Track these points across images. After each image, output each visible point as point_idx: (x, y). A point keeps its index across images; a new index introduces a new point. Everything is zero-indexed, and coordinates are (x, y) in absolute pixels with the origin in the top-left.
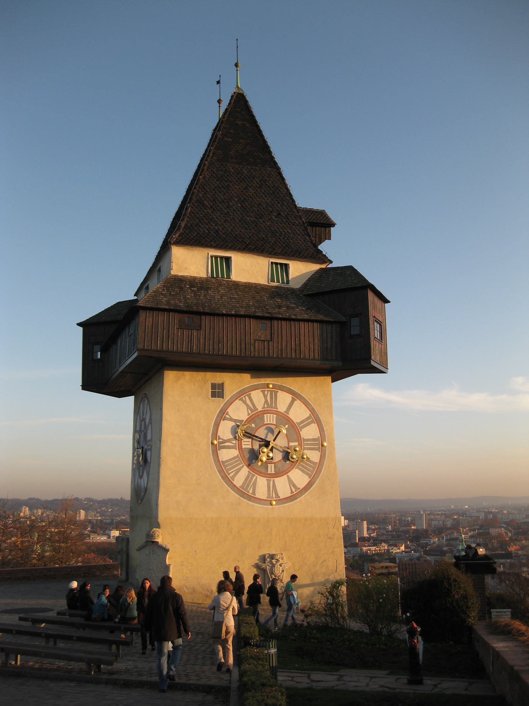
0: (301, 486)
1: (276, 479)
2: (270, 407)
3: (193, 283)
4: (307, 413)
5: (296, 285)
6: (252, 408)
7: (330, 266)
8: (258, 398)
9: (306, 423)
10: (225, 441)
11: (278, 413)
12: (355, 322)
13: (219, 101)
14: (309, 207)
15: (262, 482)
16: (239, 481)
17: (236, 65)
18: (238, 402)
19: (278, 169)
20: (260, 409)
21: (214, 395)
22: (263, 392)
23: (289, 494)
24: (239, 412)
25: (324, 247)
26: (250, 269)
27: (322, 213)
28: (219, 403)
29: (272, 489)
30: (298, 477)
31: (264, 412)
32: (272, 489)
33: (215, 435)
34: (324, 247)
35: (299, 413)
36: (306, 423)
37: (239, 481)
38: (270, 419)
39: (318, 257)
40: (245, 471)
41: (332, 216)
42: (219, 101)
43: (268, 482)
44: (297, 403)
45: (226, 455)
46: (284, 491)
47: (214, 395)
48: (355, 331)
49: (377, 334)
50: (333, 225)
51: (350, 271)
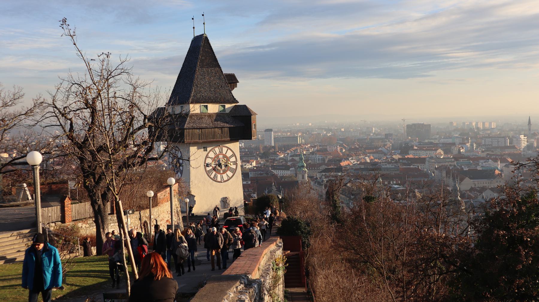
0: (230, 176)
2: (221, 152)
3: (196, 115)
4: (232, 153)
5: (227, 111)
6: (215, 154)
7: (238, 104)
8: (217, 150)
9: (231, 156)
11: (223, 154)
13: (194, 28)
14: (228, 73)
15: (219, 176)
17: (204, 24)
18: (211, 152)
19: (220, 68)
21: (204, 150)
23: (227, 179)
24: (212, 155)
25: (235, 92)
26: (214, 108)
28: (206, 153)
30: (230, 174)
34: (235, 92)
35: (229, 154)
36: (231, 156)
37: (212, 176)
38: (221, 156)
39: (234, 101)
40: (214, 173)
44: (229, 150)
46: (225, 178)
47: (204, 150)
51: (245, 107)
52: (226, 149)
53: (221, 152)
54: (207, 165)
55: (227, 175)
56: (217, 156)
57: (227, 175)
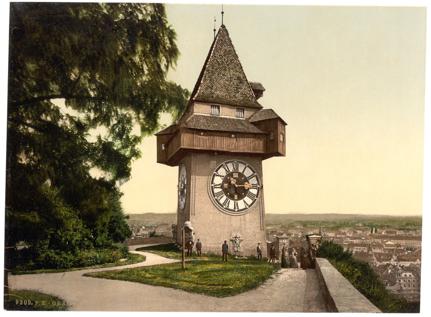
1: (238, 201)
2: (236, 170)
10: (217, 185)
12: (272, 134)
13: (215, 30)
15: (232, 202)
16: (222, 201)
17: (223, 13)
20: (231, 171)
22: (233, 164)
23: (244, 207)
24: (222, 172)
27: (260, 85)
29: (236, 205)
31: (232, 173)
32: (236, 205)
33: (212, 183)
35: (248, 173)
40: (225, 197)
41: (264, 86)
42: (215, 30)
43: (235, 202)
45: (216, 191)
48: (272, 138)
49: (282, 140)
50: (264, 90)
52: (244, 166)
53: (236, 170)
54: (216, 186)
55: (244, 202)
56: (230, 175)
57: (244, 202)
